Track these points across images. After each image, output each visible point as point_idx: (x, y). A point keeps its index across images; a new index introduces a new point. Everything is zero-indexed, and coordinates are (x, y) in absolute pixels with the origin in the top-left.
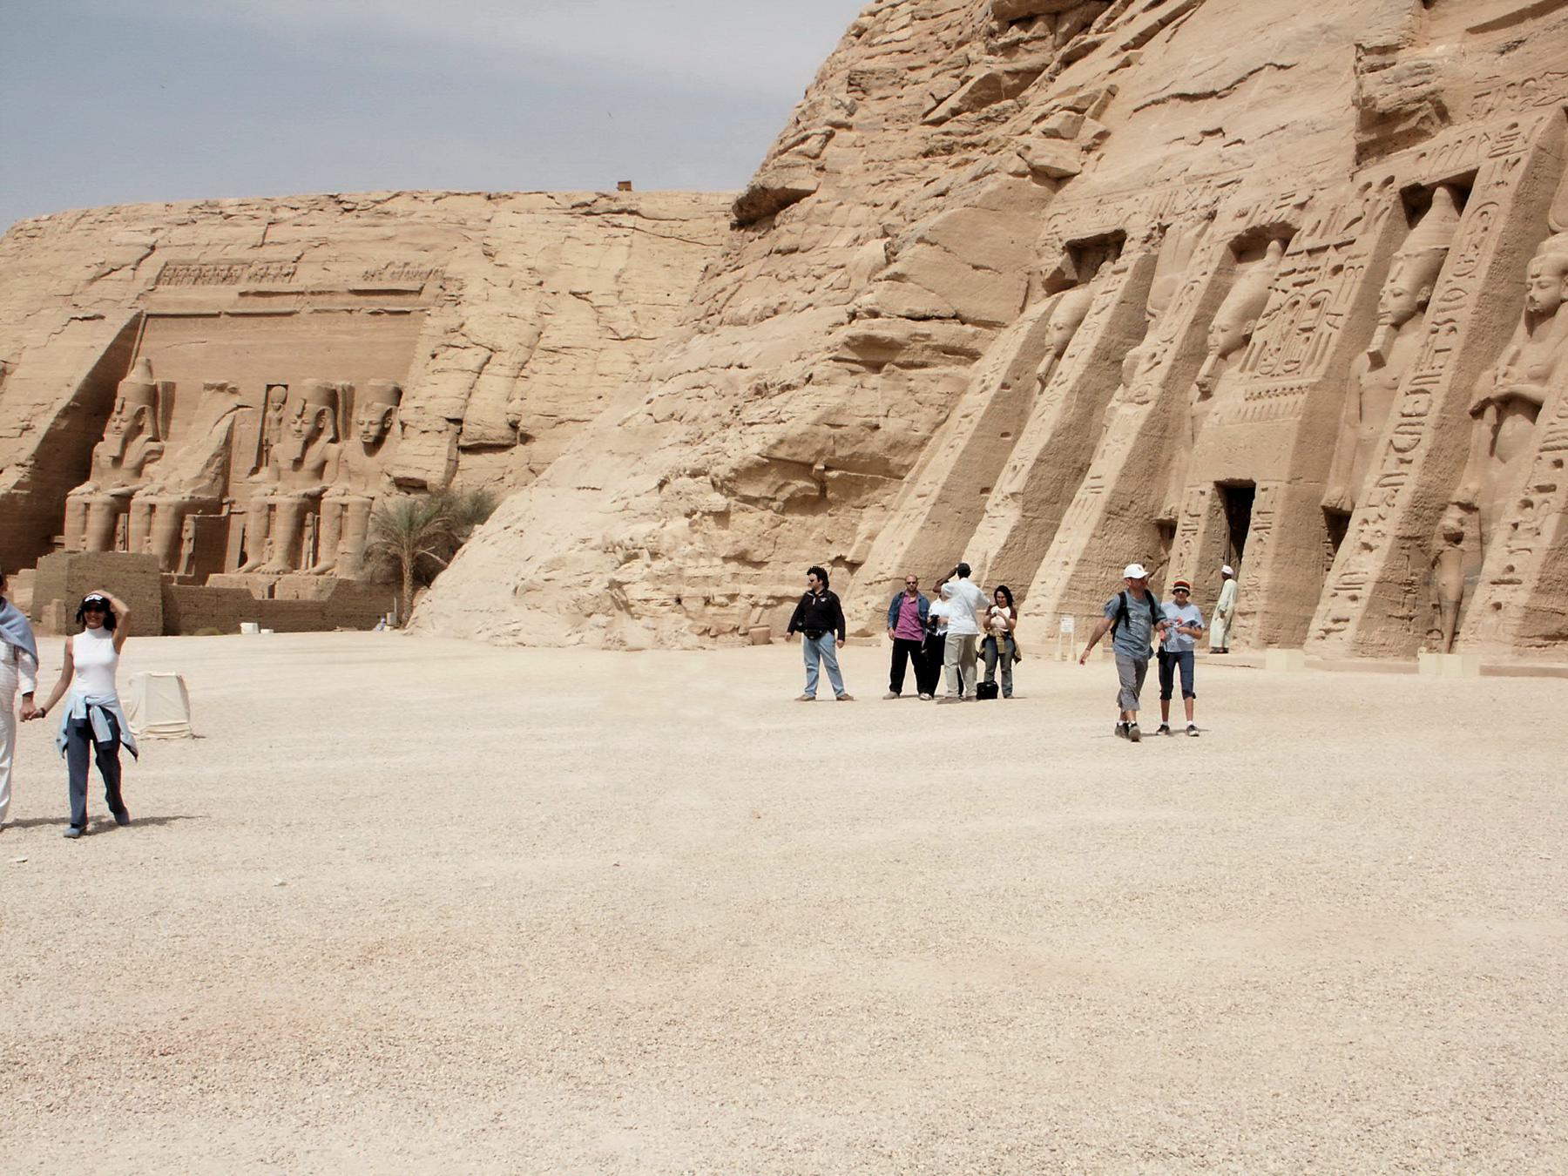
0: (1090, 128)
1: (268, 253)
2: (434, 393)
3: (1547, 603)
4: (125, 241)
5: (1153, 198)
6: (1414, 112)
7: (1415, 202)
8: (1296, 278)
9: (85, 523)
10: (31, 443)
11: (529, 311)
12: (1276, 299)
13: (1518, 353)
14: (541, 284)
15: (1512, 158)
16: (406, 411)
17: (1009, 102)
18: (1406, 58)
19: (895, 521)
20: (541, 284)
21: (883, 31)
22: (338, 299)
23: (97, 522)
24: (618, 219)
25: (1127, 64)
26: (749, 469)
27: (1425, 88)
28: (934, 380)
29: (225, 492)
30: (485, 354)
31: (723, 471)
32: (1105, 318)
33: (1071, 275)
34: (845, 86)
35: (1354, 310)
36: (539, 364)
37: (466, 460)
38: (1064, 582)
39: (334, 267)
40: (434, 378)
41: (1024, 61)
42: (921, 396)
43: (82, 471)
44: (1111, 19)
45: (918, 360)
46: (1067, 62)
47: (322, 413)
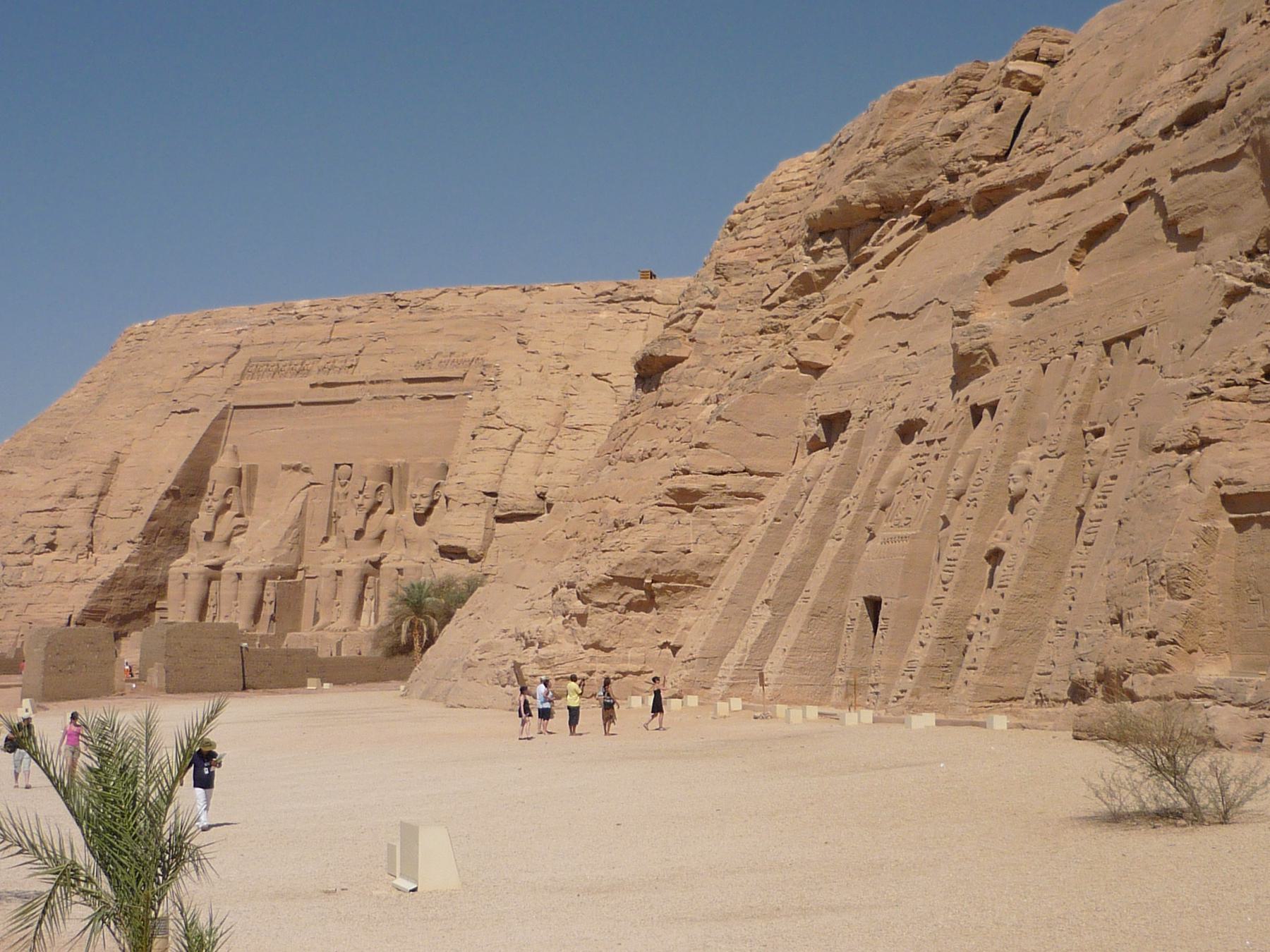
0: (845, 329)
1: (334, 347)
2: (475, 470)
3: (991, 681)
4: (215, 342)
7: (976, 414)
9: (184, 590)
10: (139, 523)
11: (556, 393)
14: (567, 368)
16: (449, 488)
17: (816, 295)
18: (977, 318)
20: (567, 368)
22: (393, 386)
23: (194, 590)
24: (635, 305)
25: (874, 280)
26: (599, 584)
28: (733, 516)
29: (300, 560)
31: (582, 586)
32: (830, 476)
33: (823, 440)
34: (713, 275)
36: (564, 441)
37: (501, 528)
40: (472, 457)
41: (827, 263)
44: (880, 237)
45: (718, 503)
46: (856, 266)
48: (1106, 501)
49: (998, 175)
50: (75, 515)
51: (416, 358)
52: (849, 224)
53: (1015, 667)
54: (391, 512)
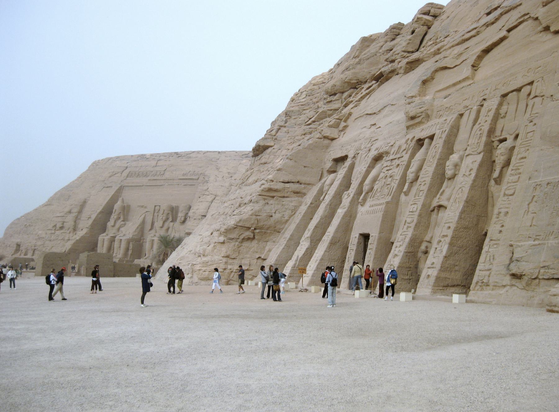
0: (343, 124)
5: (357, 144)
6: (419, 116)
8: (388, 168)
10: (90, 222)
11: (227, 184)
12: (382, 175)
13: (444, 191)
14: (231, 177)
15: (444, 129)
16: (190, 214)
19: (277, 246)
20: (231, 177)
21: (298, 100)
23: (106, 244)
25: (356, 106)
26: (230, 229)
27: (423, 109)
30: (214, 197)
35: (401, 179)
38: (315, 266)
39: (174, 172)
42: (286, 207)
43: (104, 229)
45: (286, 195)
47: (168, 214)
48: (519, 171)
49: (416, 56)
50: (70, 219)
51: (183, 173)
52: (342, 91)
53: (457, 268)
54: (171, 222)
